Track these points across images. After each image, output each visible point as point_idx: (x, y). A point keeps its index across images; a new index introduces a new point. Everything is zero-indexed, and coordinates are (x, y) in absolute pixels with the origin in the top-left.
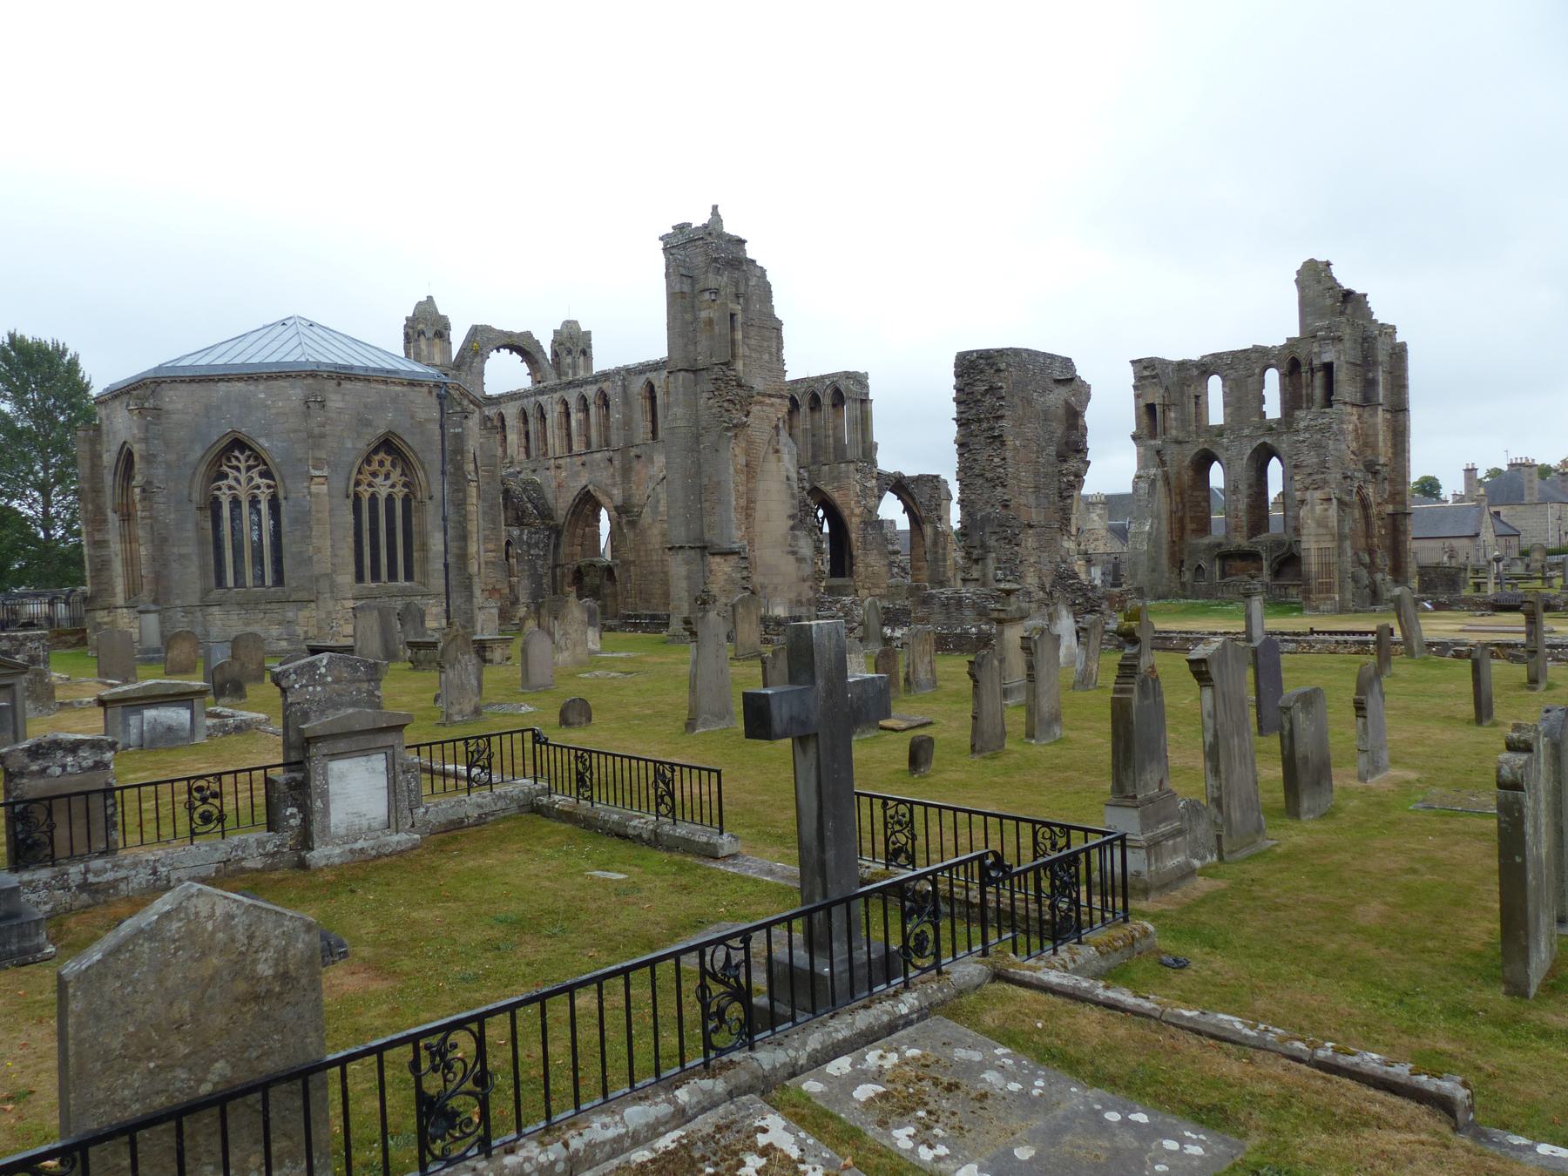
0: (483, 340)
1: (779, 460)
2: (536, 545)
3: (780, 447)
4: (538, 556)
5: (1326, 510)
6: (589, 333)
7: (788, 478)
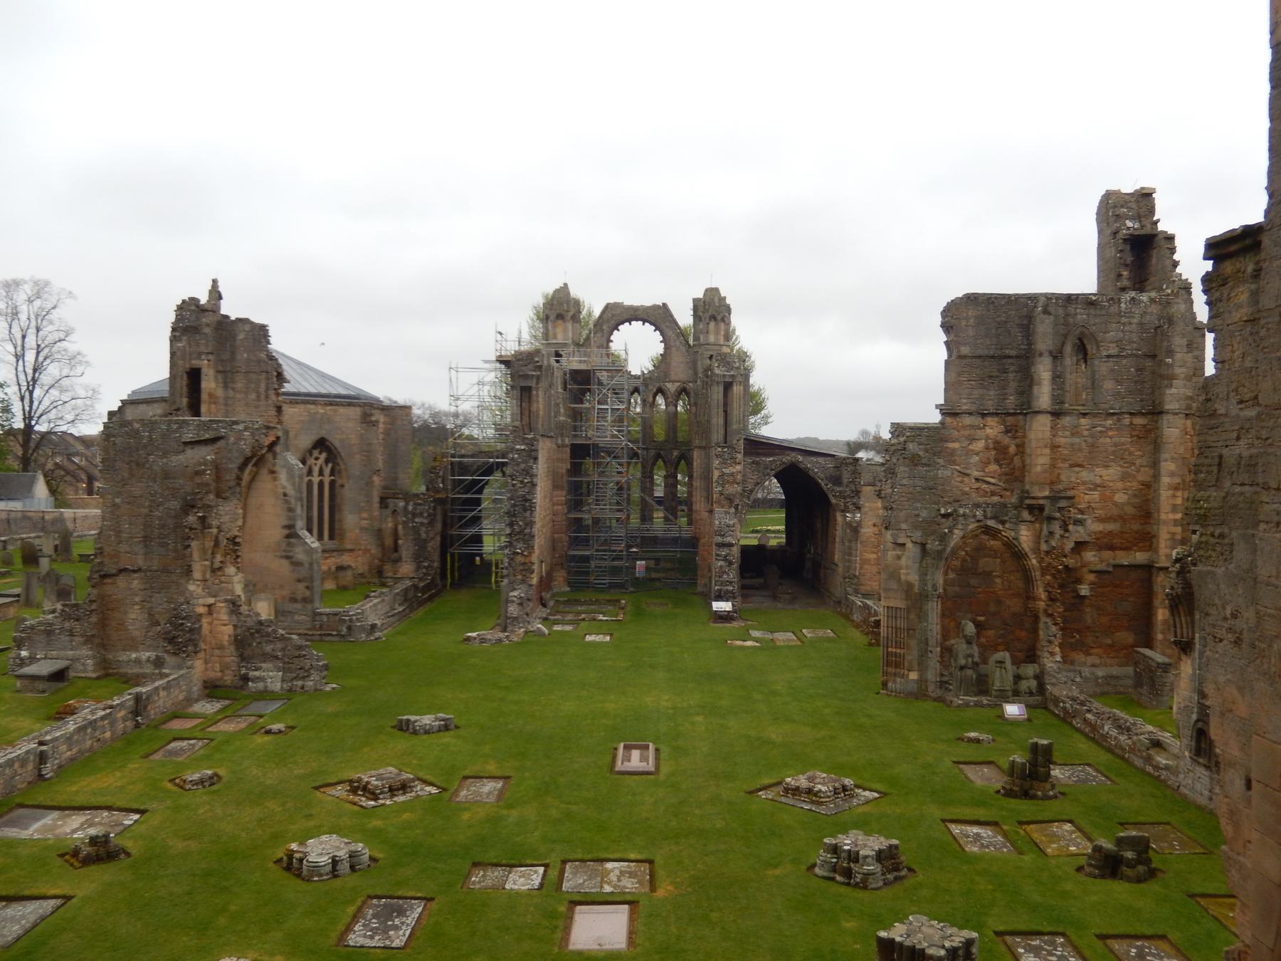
0: (617, 316)
1: (275, 479)
2: (421, 514)
3: (277, 468)
4: (422, 524)
5: (899, 558)
6: (725, 298)
7: (285, 495)
